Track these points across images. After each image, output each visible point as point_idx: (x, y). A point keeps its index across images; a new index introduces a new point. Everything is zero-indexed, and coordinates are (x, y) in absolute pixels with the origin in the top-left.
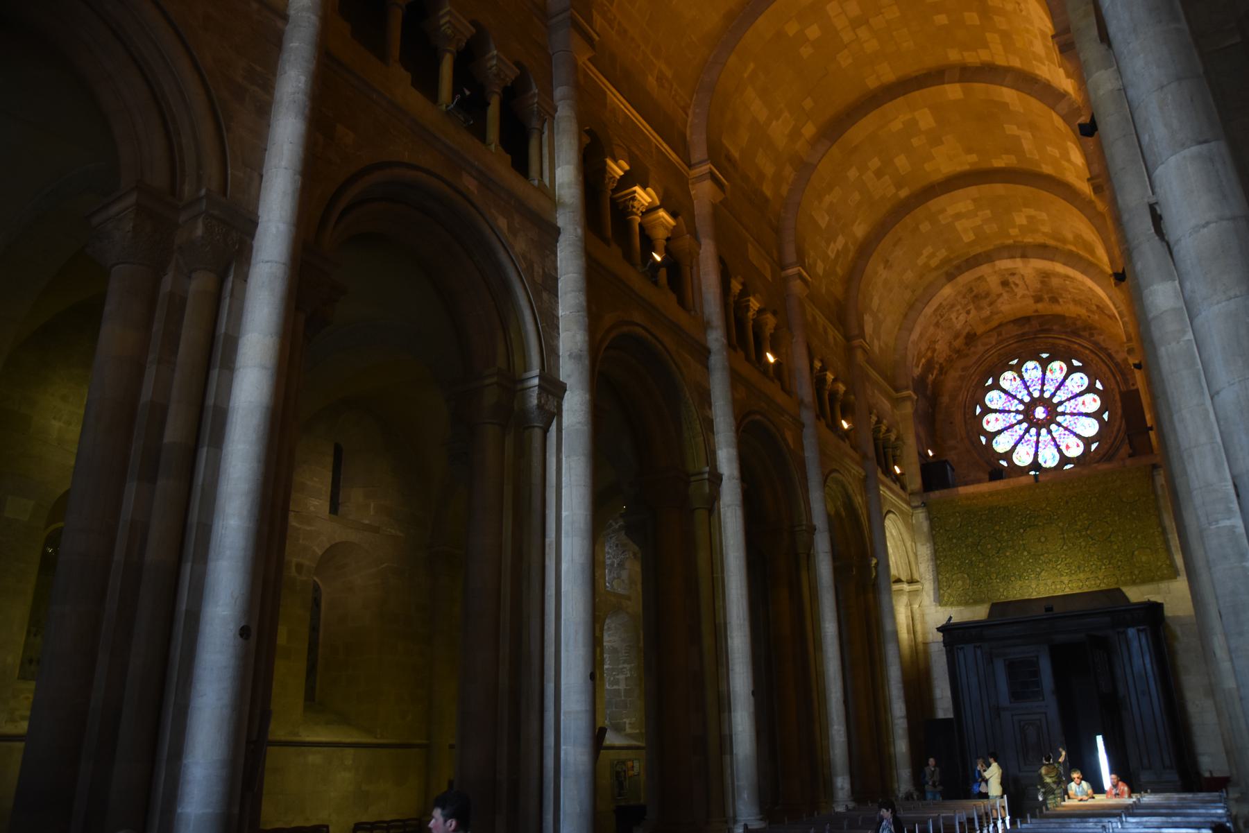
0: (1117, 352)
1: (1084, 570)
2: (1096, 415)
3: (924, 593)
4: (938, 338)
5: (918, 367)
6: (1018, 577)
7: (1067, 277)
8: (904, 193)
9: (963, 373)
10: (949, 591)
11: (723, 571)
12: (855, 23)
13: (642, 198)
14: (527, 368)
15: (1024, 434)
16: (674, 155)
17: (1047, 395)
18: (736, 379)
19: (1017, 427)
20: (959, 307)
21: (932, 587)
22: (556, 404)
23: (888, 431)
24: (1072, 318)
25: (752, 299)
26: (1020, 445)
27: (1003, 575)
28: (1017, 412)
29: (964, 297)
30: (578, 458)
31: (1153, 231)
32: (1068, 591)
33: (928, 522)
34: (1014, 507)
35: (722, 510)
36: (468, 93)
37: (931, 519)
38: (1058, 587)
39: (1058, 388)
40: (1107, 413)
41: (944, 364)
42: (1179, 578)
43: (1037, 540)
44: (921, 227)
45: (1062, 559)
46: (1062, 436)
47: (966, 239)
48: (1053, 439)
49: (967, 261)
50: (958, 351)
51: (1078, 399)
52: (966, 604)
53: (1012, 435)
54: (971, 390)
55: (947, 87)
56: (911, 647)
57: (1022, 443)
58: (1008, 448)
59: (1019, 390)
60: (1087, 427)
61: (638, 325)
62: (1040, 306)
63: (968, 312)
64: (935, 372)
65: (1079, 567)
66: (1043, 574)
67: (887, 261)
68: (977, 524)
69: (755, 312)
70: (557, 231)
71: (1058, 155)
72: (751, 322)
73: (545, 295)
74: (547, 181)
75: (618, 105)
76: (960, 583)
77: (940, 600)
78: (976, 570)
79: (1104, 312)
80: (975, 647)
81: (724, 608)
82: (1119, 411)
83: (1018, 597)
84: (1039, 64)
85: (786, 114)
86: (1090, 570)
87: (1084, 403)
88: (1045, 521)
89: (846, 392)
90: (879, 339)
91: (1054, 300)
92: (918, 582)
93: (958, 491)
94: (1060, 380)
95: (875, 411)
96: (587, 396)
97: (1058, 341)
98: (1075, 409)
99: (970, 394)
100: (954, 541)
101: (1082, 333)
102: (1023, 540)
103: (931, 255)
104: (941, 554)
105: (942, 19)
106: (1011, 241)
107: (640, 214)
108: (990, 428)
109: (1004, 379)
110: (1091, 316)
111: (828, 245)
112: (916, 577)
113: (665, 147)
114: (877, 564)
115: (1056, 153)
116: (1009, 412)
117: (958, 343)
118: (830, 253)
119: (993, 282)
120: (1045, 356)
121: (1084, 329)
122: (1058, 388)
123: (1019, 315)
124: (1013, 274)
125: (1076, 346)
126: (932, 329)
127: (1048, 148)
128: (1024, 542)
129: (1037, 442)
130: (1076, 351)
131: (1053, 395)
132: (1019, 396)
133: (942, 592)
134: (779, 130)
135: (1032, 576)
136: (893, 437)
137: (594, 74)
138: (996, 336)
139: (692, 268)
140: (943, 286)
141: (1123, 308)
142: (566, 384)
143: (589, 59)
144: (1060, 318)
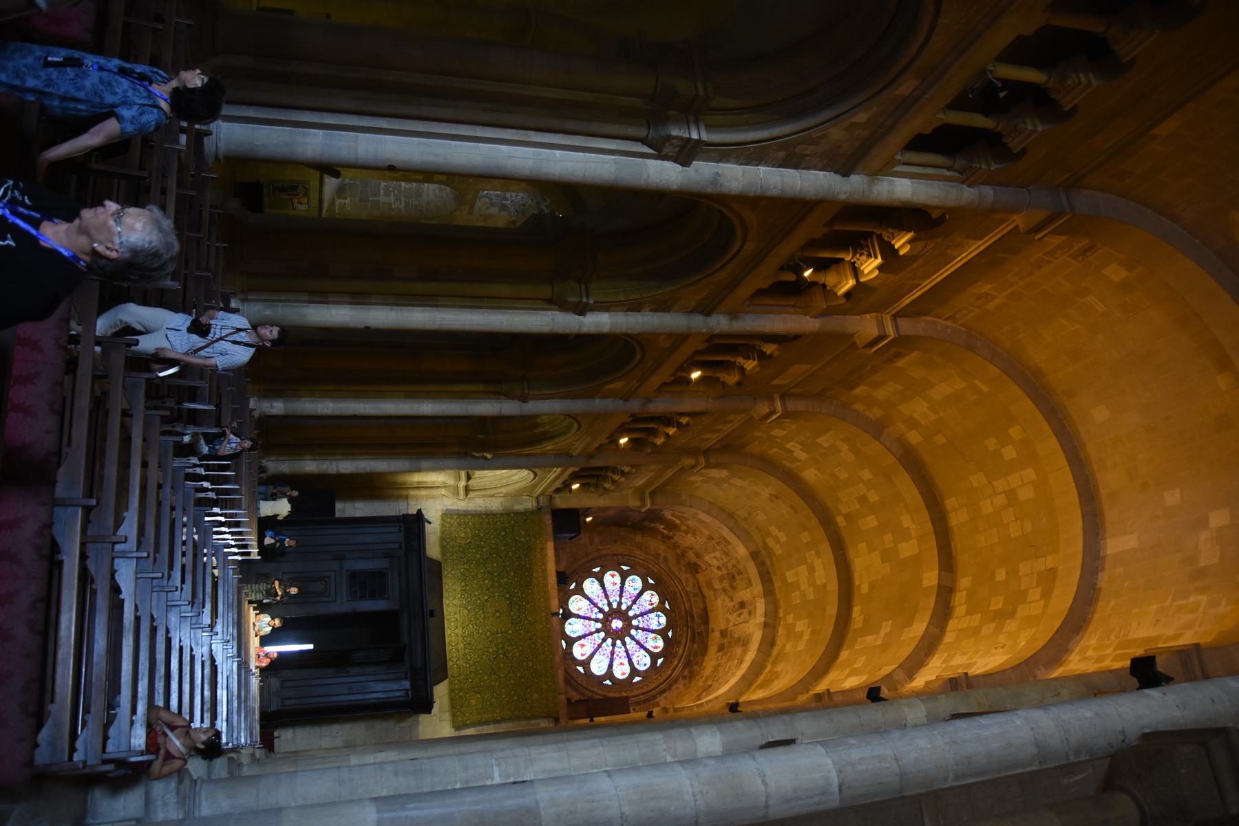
0: (666, 698)
2: (609, 674)
3: (456, 500)
4: (698, 538)
5: (672, 516)
6: (464, 588)
7: (741, 662)
8: (840, 521)
9: (661, 558)
10: (455, 524)
11: (487, 308)
12: (1011, 494)
13: (868, 265)
14: (710, 127)
15: (598, 608)
16: (907, 302)
17: (633, 632)
18: (680, 338)
19: (605, 602)
20: (725, 560)
21: (460, 508)
22: (670, 154)
23: (614, 482)
24: (702, 663)
25: (755, 363)
26: (588, 602)
27: (467, 575)
28: (620, 603)
29: (734, 566)
30: (613, 171)
31: (771, 740)
32: (448, 632)
33: (523, 511)
34: (530, 591)
35: (550, 312)
36: (1002, 95)
37: (525, 514)
38: (452, 624)
39: (638, 643)
40: (610, 684)
41: (672, 540)
42: (453, 730)
44: (806, 533)
46: (593, 642)
47: (788, 574)
48: (591, 634)
50: (683, 555)
51: (627, 660)
52: (442, 539)
53: (598, 596)
54: (645, 563)
55: (937, 572)
56: (405, 483)
57: (590, 605)
58: (587, 591)
60: (600, 665)
61: (742, 247)
62: (717, 634)
63: (719, 568)
64: (666, 532)
65: (469, 644)
66: (465, 611)
67: (777, 498)
68: (517, 556)
69: (742, 364)
70: (846, 174)
71: (855, 666)
72: (733, 360)
73: (782, 154)
74: (899, 168)
75: (966, 251)
76: (463, 535)
77: (447, 514)
79: (705, 690)
80: (401, 543)
81: (453, 306)
82: (611, 695)
83: (445, 587)
84: (943, 658)
85: (933, 417)
87: (622, 664)
88: (514, 618)
89: (654, 445)
90: (701, 481)
91: (721, 648)
92: (467, 495)
93: (549, 541)
94: (645, 645)
95: (634, 470)
96: (675, 187)
98: (618, 655)
99: (641, 561)
100: (503, 533)
101: (687, 670)
102: (498, 596)
103: (778, 540)
104: (491, 520)
105: (1001, 575)
106: (781, 615)
107: (852, 261)
108: (608, 578)
109: (653, 595)
111: (801, 443)
112: (471, 494)
113: (917, 294)
114: (486, 458)
115: (858, 665)
116: (621, 596)
117: (691, 556)
118: (792, 443)
119: (744, 594)
120: (670, 634)
121: (691, 672)
122: (638, 643)
123: (710, 614)
124: (750, 613)
125: (676, 663)
126: (707, 532)
127: (864, 658)
129: (589, 619)
130: (671, 662)
131: (633, 638)
132: (634, 607)
133: (455, 517)
134: (918, 408)
135: (464, 602)
136: (607, 485)
137: (1003, 229)
138: (695, 591)
139: (793, 306)
140: (746, 547)
141: (706, 708)
142: (689, 167)
143: (1017, 227)
144: (704, 651)
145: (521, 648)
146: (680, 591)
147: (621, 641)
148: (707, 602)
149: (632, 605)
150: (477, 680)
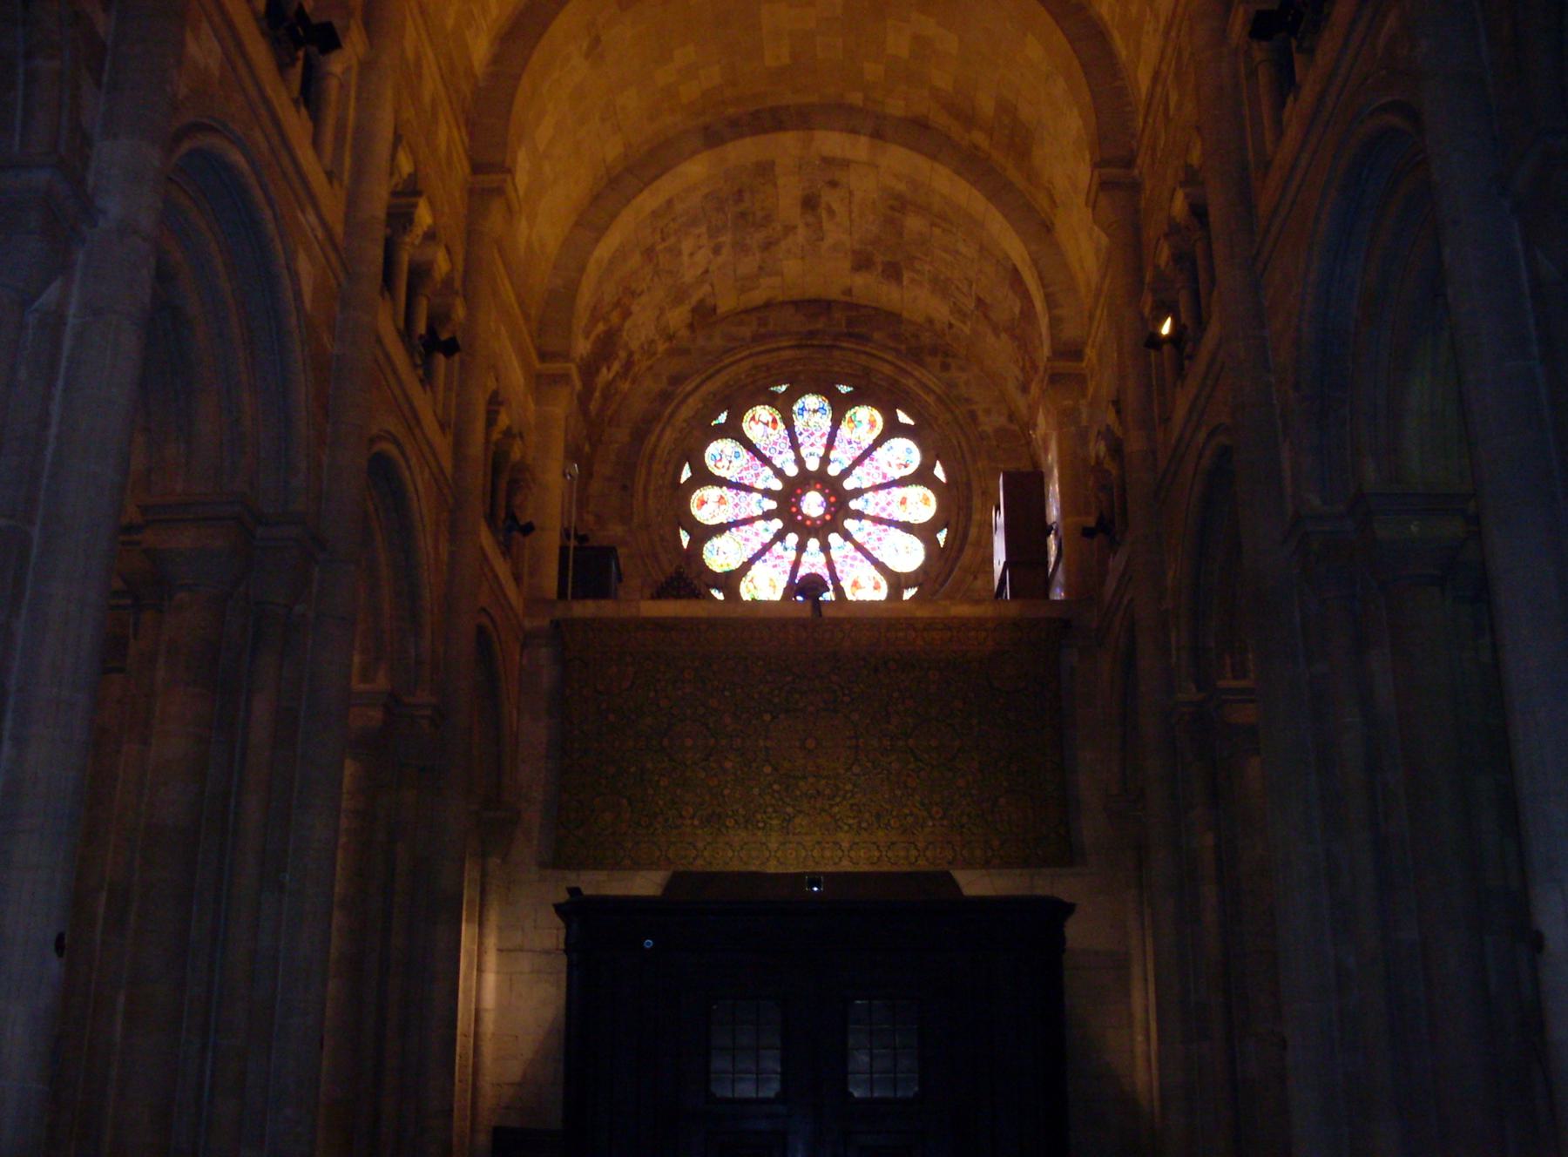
0: (988, 412)
1: (888, 824)
2: (923, 532)
6: (742, 820)
15: (772, 542)
20: (703, 229)
32: (846, 866)
38: (828, 854)
39: (858, 461)
40: (945, 531)
41: (636, 357)
43: (797, 744)
45: (846, 792)
46: (849, 561)
50: (670, 338)
51: (894, 490)
57: (765, 561)
58: (734, 565)
59: (778, 448)
62: (859, 281)
63: (717, 250)
64: (616, 366)
65: (878, 816)
66: (797, 821)
67: (596, 41)
78: (651, 791)
79: (986, 317)
83: (736, 866)
86: (901, 825)
87: (903, 502)
89: (448, 282)
91: (893, 272)
94: (865, 445)
98: (884, 509)
109: (753, 418)
116: (749, 489)
117: (677, 317)
120: (844, 389)
122: (858, 461)
123: (807, 296)
124: (833, 184)
126: (635, 260)
128: (769, 744)
131: (846, 473)
132: (777, 462)
135: (775, 822)
140: (694, 153)
144: (892, 318)
145: (896, 695)
146: (751, 355)
147: (852, 498)
148: (781, 298)
149: (773, 467)
150: (964, 803)
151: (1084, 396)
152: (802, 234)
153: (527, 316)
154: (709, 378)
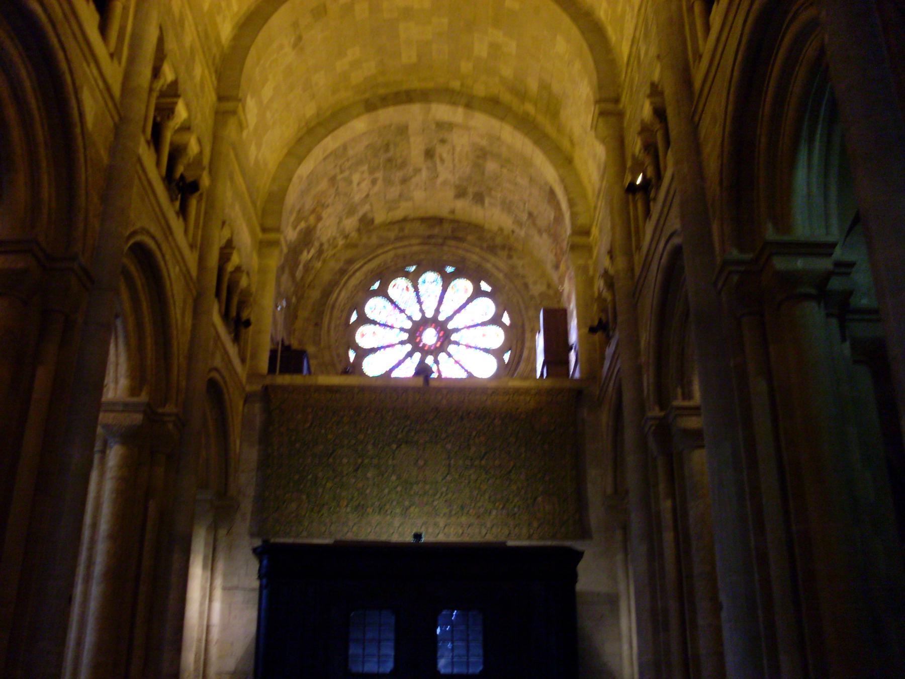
0: (535, 283)
20: (365, 168)
32: (441, 538)
41: (326, 247)
47: (405, 60)
49: (397, 94)
50: (346, 237)
62: (460, 204)
64: (313, 251)
66: (412, 509)
67: (300, 38)
91: (479, 198)
97: (468, 255)
110: (517, 230)
117: (351, 224)
122: (458, 311)
124: (443, 141)
126: (324, 184)
140: (358, 115)
144: (478, 229)
151: (591, 257)
152: (424, 174)
153: (254, 203)
154: (369, 261)
